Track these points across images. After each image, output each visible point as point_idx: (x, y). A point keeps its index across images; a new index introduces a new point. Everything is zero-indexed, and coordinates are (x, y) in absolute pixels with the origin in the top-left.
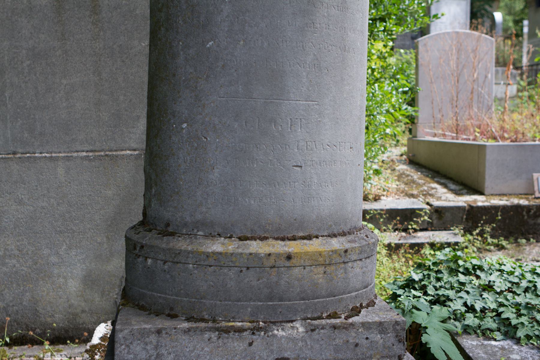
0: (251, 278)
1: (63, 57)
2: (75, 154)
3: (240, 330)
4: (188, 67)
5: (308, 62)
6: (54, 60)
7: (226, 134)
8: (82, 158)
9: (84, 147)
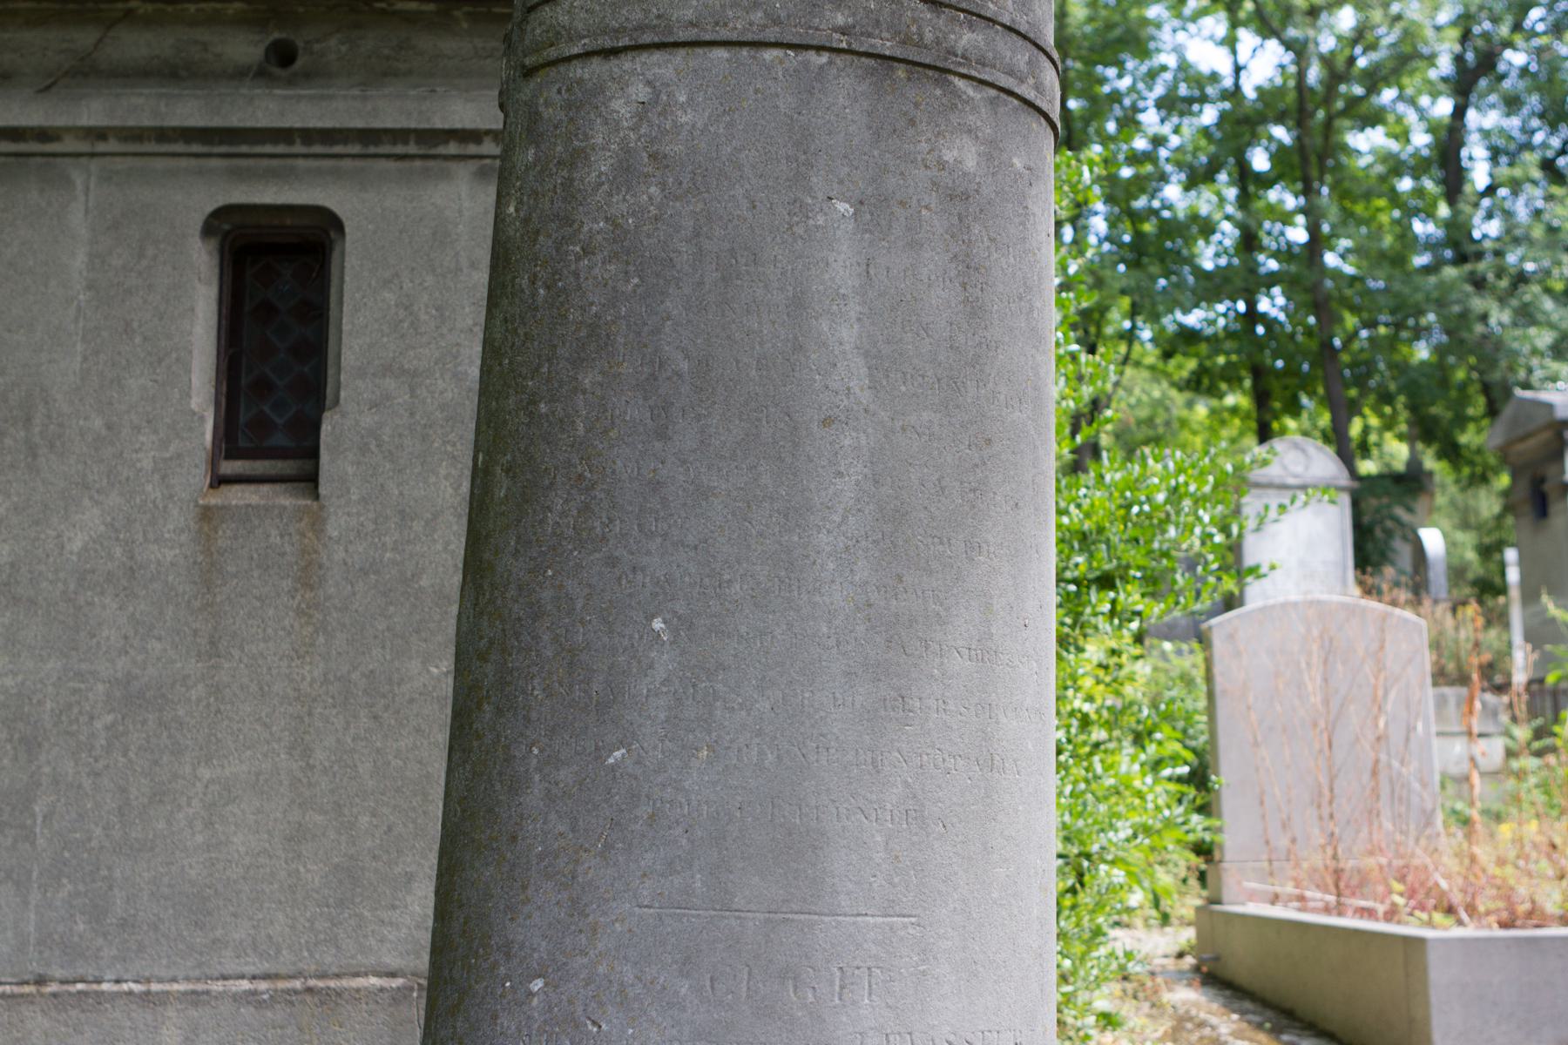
1: (208, 705)
2: (217, 987)
4: (553, 816)
5: (889, 806)
6: (181, 713)
7: (654, 1014)
9: (247, 964)
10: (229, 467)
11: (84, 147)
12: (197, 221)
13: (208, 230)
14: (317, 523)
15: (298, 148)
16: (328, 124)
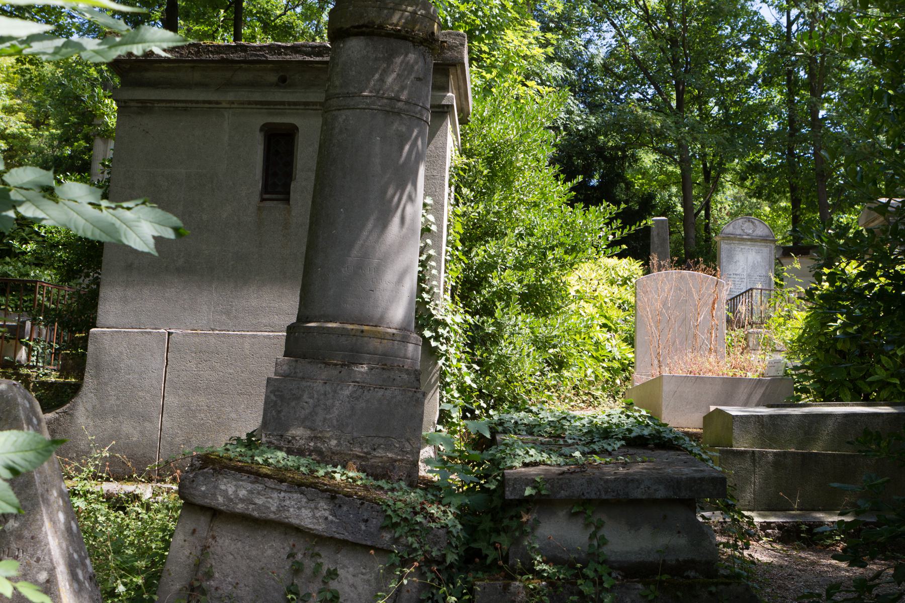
0: (343, 341)
3: (336, 365)
8: (264, 337)
11: (228, 106)
12: (258, 127)
13: (261, 130)
15: (287, 107)
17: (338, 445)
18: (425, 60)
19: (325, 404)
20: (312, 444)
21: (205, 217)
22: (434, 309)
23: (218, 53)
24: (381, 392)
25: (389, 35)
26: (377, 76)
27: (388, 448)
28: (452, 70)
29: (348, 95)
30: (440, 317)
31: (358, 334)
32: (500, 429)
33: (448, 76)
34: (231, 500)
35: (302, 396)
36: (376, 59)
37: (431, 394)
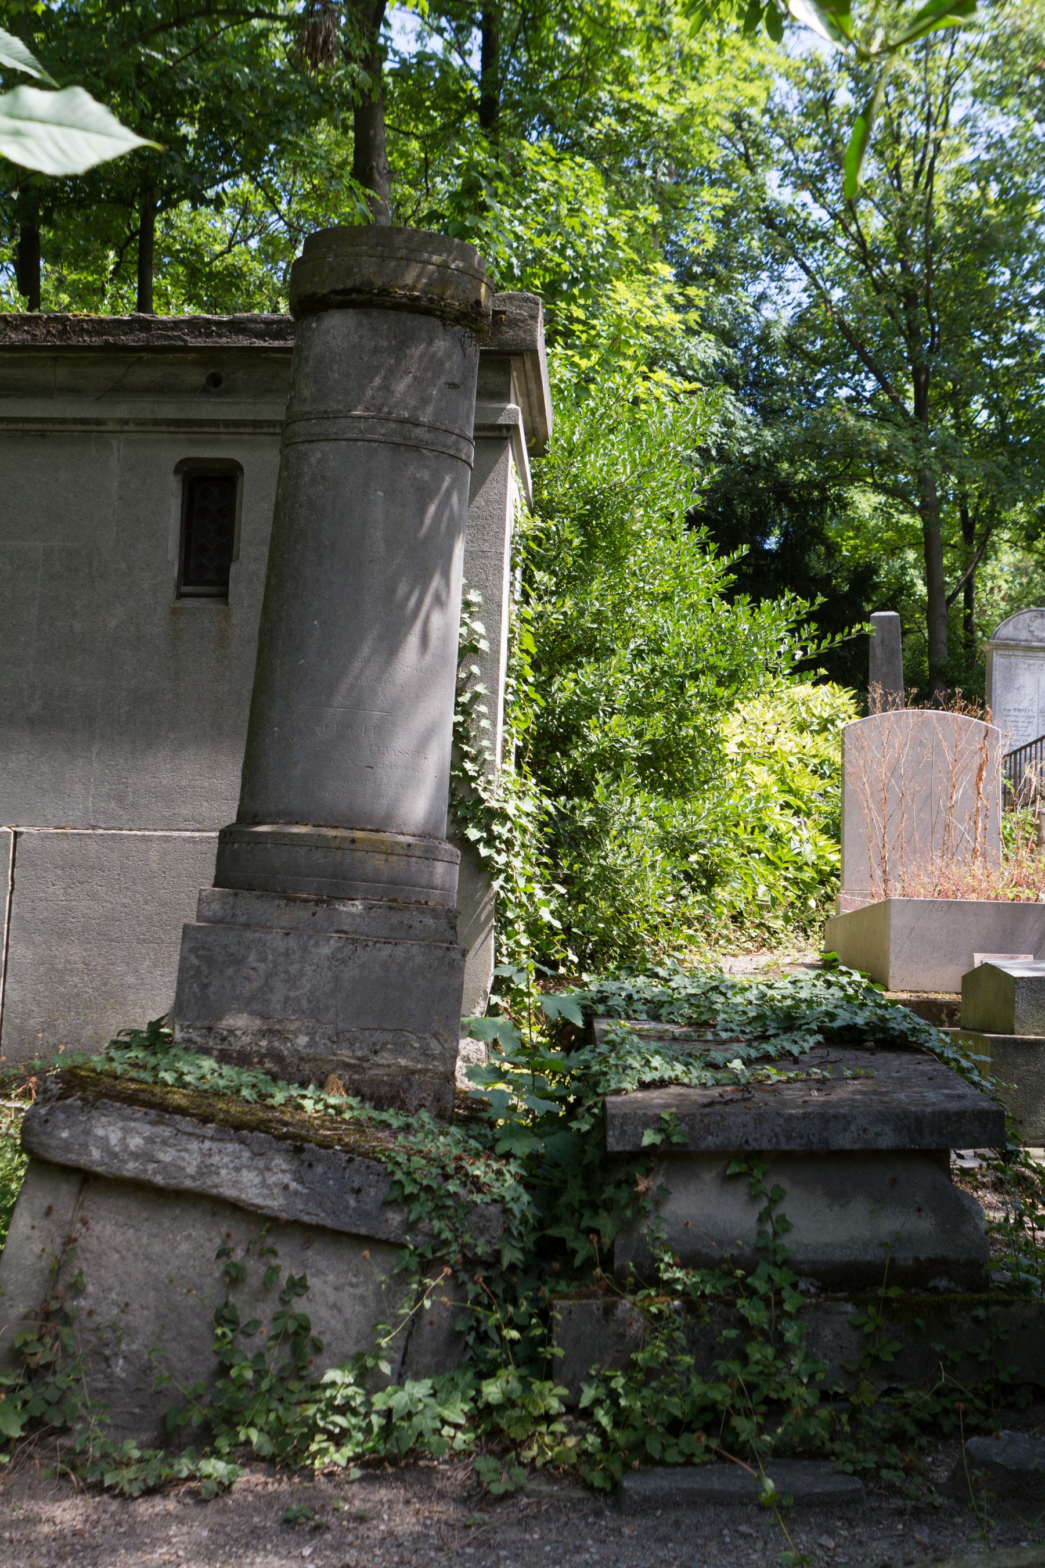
0: (318, 857)
2: (176, 834)
3: (306, 901)
8: (184, 839)
10: (185, 589)
11: (118, 428)
13: (177, 471)
14: (227, 617)
15: (222, 429)
16: (236, 417)
17: (312, 1043)
18: (464, 350)
19: (287, 972)
20: (264, 1043)
21: (78, 626)
22: (485, 789)
23: (99, 334)
24: (387, 950)
25: (398, 307)
26: (377, 381)
27: (400, 1049)
28: (515, 363)
29: (325, 416)
30: (494, 804)
31: (347, 845)
32: (601, 1008)
33: (508, 373)
34: (115, 1155)
35: (245, 957)
36: (376, 350)
37: (479, 940)
